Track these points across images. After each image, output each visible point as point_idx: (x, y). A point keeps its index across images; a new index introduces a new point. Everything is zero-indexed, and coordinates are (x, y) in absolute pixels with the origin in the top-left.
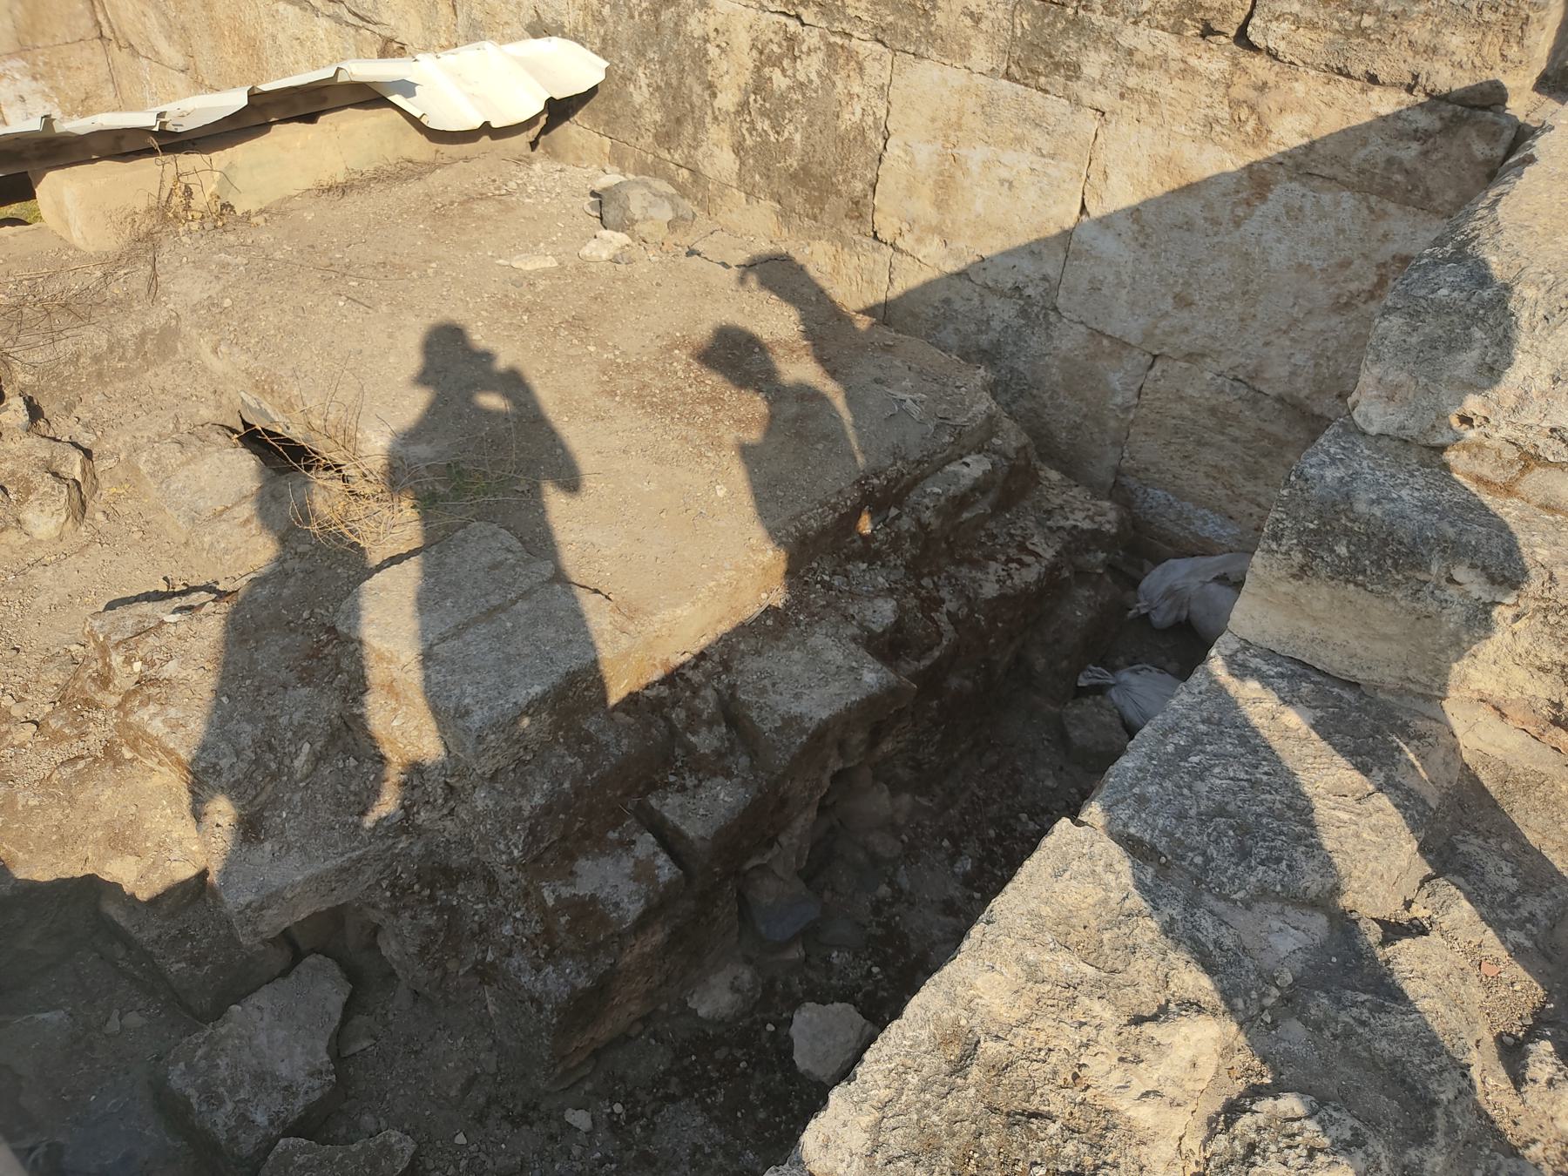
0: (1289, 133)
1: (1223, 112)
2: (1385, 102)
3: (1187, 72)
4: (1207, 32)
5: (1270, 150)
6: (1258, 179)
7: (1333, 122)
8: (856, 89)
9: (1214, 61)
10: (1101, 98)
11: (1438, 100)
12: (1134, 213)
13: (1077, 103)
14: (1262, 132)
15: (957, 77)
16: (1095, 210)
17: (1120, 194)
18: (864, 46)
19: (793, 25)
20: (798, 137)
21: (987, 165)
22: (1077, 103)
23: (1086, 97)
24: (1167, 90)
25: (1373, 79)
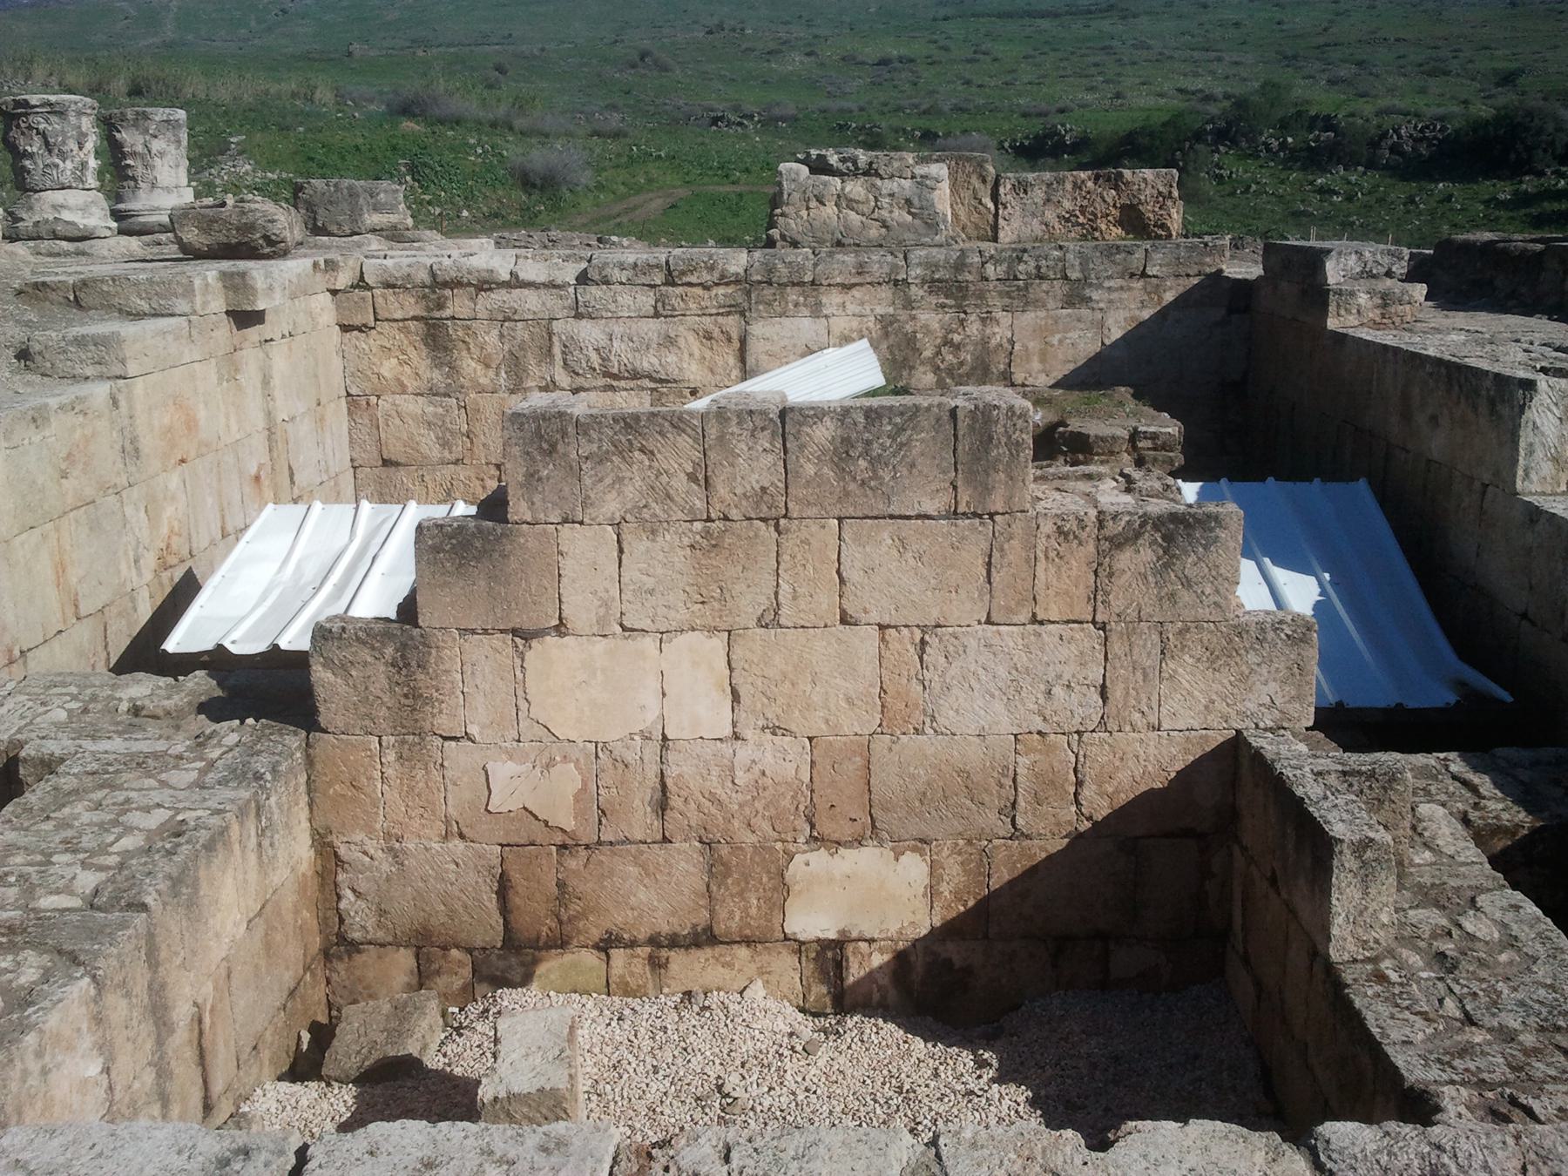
0: (1169, 297)
1: (1146, 297)
2: (1195, 281)
3: (1130, 289)
4: (1132, 275)
5: (1164, 303)
6: (1163, 314)
7: (1181, 290)
8: (996, 330)
9: (1138, 284)
10: (1102, 305)
11: (1208, 276)
12: (1123, 337)
13: (1093, 309)
14: (1160, 299)
15: (1042, 314)
16: (1108, 342)
17: (1116, 334)
18: (999, 314)
19: (962, 315)
20: (969, 357)
21: (1060, 341)
22: (1093, 309)
23: (1095, 306)
24: (1125, 295)
25: (1188, 275)
